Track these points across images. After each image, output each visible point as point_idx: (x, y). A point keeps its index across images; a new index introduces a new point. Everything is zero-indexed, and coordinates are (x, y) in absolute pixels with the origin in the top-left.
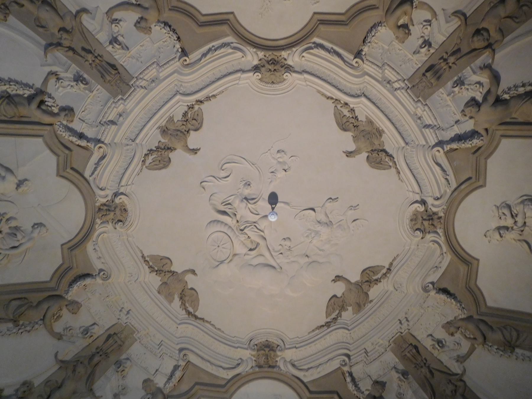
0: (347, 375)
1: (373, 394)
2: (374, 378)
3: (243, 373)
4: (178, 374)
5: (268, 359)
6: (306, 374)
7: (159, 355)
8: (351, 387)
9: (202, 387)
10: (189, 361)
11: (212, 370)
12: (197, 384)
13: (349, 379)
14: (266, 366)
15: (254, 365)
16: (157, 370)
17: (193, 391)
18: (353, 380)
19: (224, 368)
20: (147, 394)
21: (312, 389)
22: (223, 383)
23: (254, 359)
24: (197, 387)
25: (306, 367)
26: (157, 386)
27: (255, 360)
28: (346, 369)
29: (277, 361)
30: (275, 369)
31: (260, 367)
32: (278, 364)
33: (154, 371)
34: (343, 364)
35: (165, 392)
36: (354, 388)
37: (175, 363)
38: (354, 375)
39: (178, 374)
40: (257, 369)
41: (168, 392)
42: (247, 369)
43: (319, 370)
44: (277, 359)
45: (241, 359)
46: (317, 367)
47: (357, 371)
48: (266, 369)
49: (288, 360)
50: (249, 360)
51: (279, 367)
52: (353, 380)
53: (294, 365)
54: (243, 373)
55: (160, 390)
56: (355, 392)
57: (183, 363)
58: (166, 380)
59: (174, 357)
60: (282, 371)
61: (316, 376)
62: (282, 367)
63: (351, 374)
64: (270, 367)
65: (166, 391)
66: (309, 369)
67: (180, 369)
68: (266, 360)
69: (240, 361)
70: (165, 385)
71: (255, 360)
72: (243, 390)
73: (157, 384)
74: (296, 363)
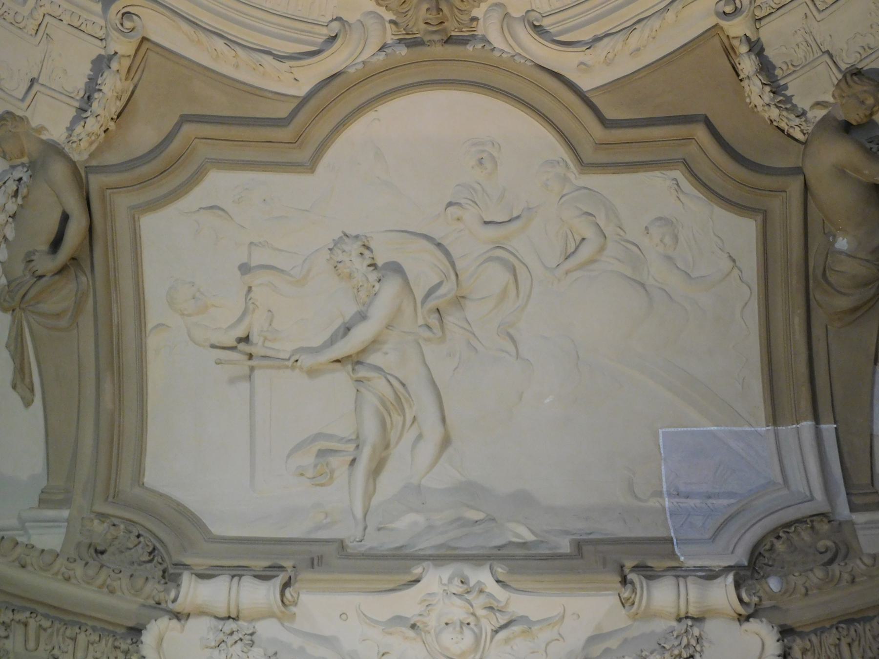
0: (744, 49)
1: (841, 115)
2: (847, 61)
3: (352, 70)
4: (112, 84)
5: (439, 10)
6: (588, 57)
7: (32, 25)
8: (756, 91)
9: (208, 130)
10: (144, 39)
11: (237, 66)
12: (185, 119)
13: (748, 65)
14: (436, 37)
15: (389, 42)
16: (33, 81)
17: (175, 146)
18: (766, 68)
19: (279, 58)
20: (13, 167)
21: (610, 114)
22: (283, 111)
23: (389, 16)
24: (188, 129)
25: (585, 35)
26: (44, 137)
27: (392, 22)
28: (737, 28)
29: (475, 19)
30: (470, 48)
31: (414, 43)
32: (479, 32)
33: (27, 84)
34: (729, 9)
35: (75, 157)
36: (768, 97)
37: (96, 50)
38: (769, 53)
39: (112, 84)
40: (403, 51)
41: (85, 156)
42: (364, 57)
43: (635, 40)
44: (475, 13)
45: (339, 19)
46: (632, 28)
47: (782, 36)
48: (438, 50)
49: (517, 14)
50: (370, 22)
51: (485, 40)
52: (766, 68)
53: (538, 30)
54: (352, 70)
55: (54, 149)
56: (774, 113)
57: (124, 46)
58: (72, 113)
59: (89, 29)
60: (497, 54)
61: (625, 67)
62: (496, 39)
63: (756, 48)
64: (449, 40)
65: (80, 154)
66: (597, 39)
67: (115, 65)
68: (432, 17)
69: (336, 25)
70: (70, 129)
71: (392, 22)
72: (358, 129)
73: (41, 129)
74: (545, 22)
